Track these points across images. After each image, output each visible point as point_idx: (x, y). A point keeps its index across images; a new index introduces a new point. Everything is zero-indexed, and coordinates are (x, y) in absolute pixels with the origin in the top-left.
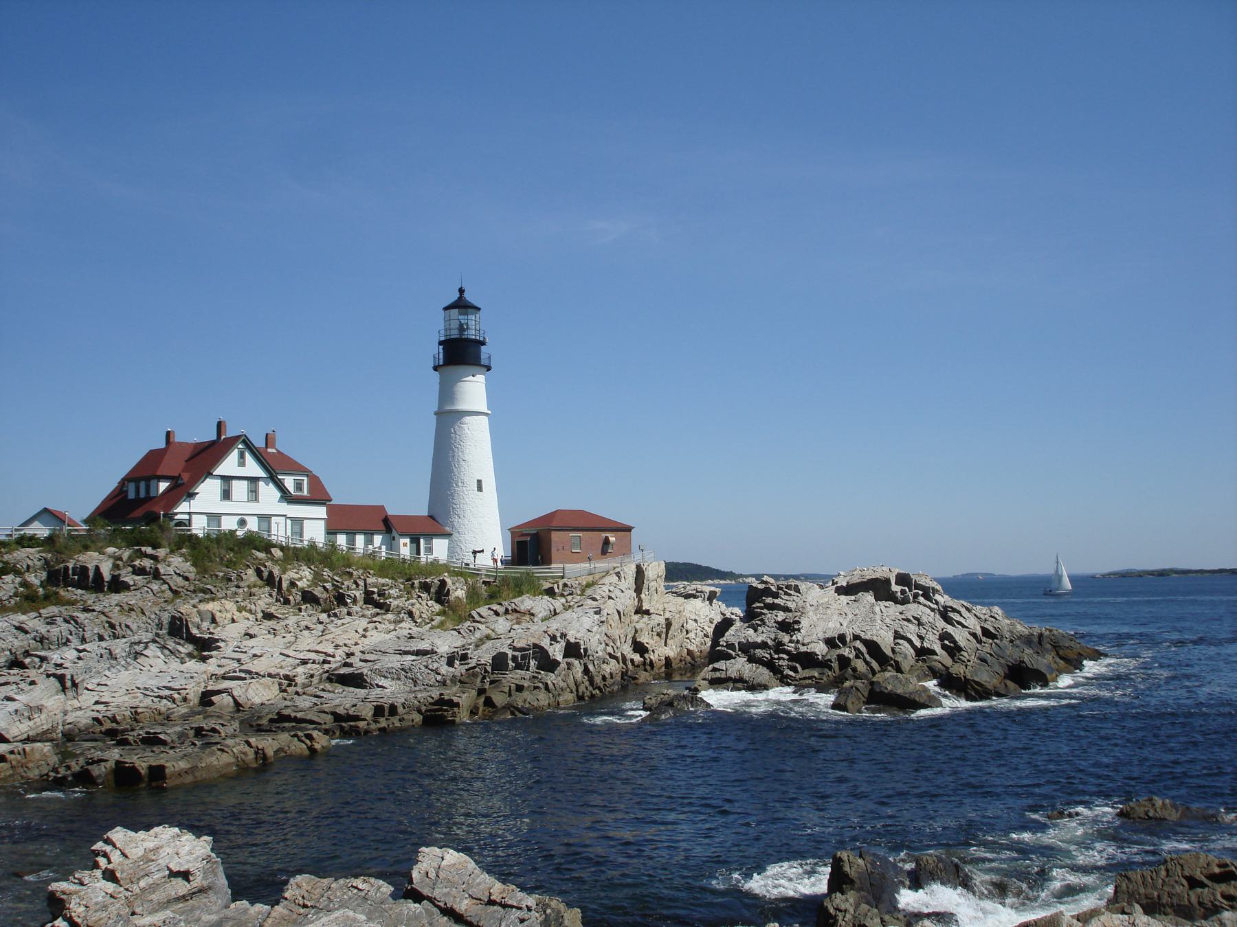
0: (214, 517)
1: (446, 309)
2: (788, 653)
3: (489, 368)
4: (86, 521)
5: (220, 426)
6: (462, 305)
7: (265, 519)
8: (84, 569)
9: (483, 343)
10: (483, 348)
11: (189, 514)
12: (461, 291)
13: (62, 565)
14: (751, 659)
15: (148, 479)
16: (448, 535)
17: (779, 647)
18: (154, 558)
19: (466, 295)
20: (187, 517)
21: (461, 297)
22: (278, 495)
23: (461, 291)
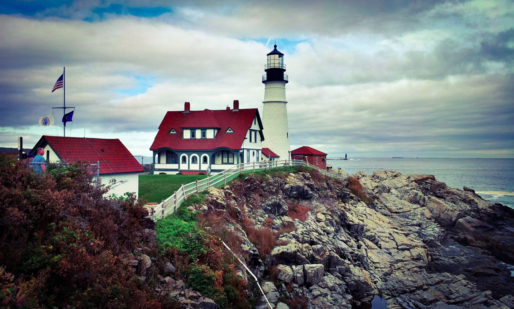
0: (248, 150)
1: (268, 55)
2: (484, 214)
3: (287, 82)
4: (151, 149)
6: (275, 52)
7: (258, 150)
8: (298, 188)
9: (285, 70)
10: (285, 73)
11: (243, 149)
12: (275, 46)
13: (287, 186)
14: (473, 217)
15: (204, 130)
16: (278, 157)
17: (478, 211)
18: (308, 179)
19: (277, 48)
20: (241, 151)
21: (275, 49)
22: (260, 139)
23: (275, 46)
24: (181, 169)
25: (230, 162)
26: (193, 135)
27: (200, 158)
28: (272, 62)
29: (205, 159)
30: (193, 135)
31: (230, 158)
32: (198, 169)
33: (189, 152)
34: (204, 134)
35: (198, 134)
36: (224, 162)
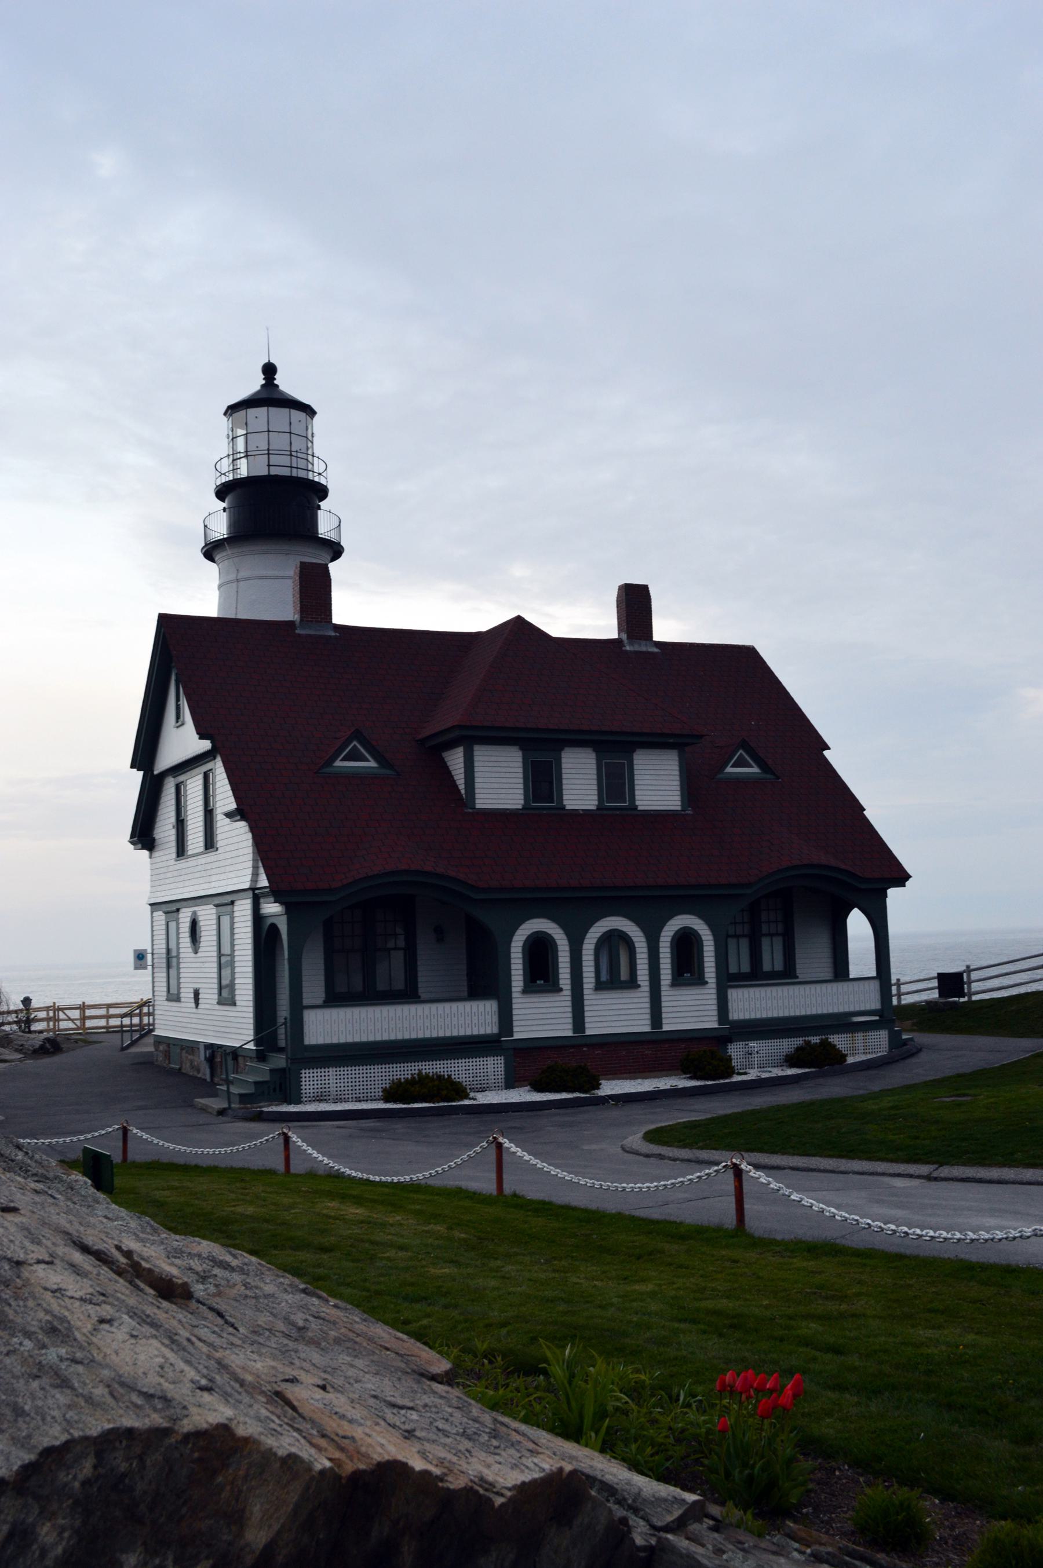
5: (635, 603)
12: (269, 370)
15: (615, 751)
19: (279, 380)
23: (269, 370)
24: (522, 1031)
25: (767, 967)
26: (542, 780)
27: (650, 949)
28: (260, 442)
29: (686, 947)
30: (542, 780)
31: (765, 942)
32: (642, 1025)
33: (576, 907)
34: (616, 782)
35: (580, 785)
36: (733, 969)
